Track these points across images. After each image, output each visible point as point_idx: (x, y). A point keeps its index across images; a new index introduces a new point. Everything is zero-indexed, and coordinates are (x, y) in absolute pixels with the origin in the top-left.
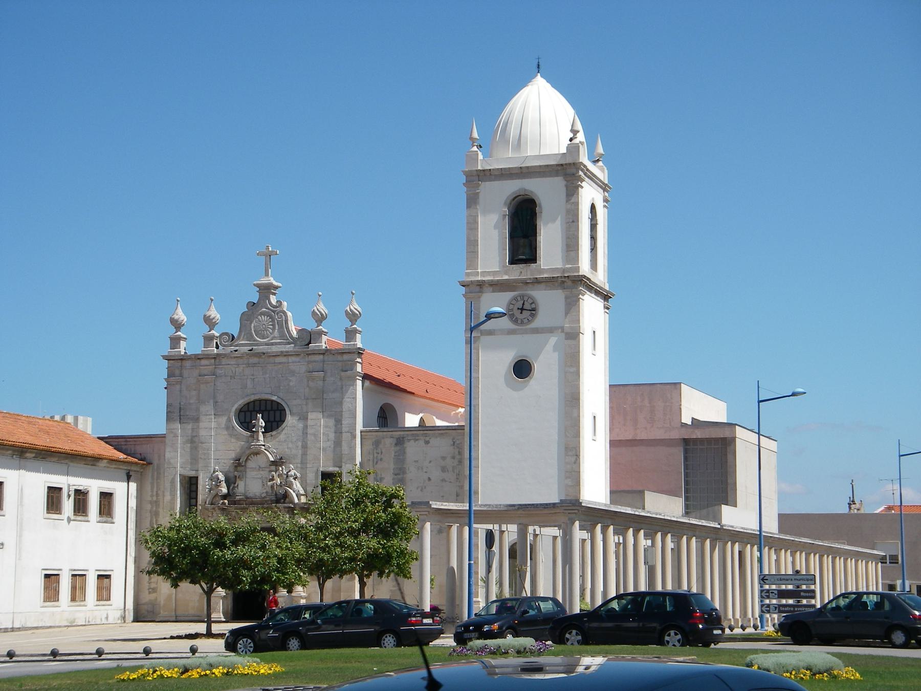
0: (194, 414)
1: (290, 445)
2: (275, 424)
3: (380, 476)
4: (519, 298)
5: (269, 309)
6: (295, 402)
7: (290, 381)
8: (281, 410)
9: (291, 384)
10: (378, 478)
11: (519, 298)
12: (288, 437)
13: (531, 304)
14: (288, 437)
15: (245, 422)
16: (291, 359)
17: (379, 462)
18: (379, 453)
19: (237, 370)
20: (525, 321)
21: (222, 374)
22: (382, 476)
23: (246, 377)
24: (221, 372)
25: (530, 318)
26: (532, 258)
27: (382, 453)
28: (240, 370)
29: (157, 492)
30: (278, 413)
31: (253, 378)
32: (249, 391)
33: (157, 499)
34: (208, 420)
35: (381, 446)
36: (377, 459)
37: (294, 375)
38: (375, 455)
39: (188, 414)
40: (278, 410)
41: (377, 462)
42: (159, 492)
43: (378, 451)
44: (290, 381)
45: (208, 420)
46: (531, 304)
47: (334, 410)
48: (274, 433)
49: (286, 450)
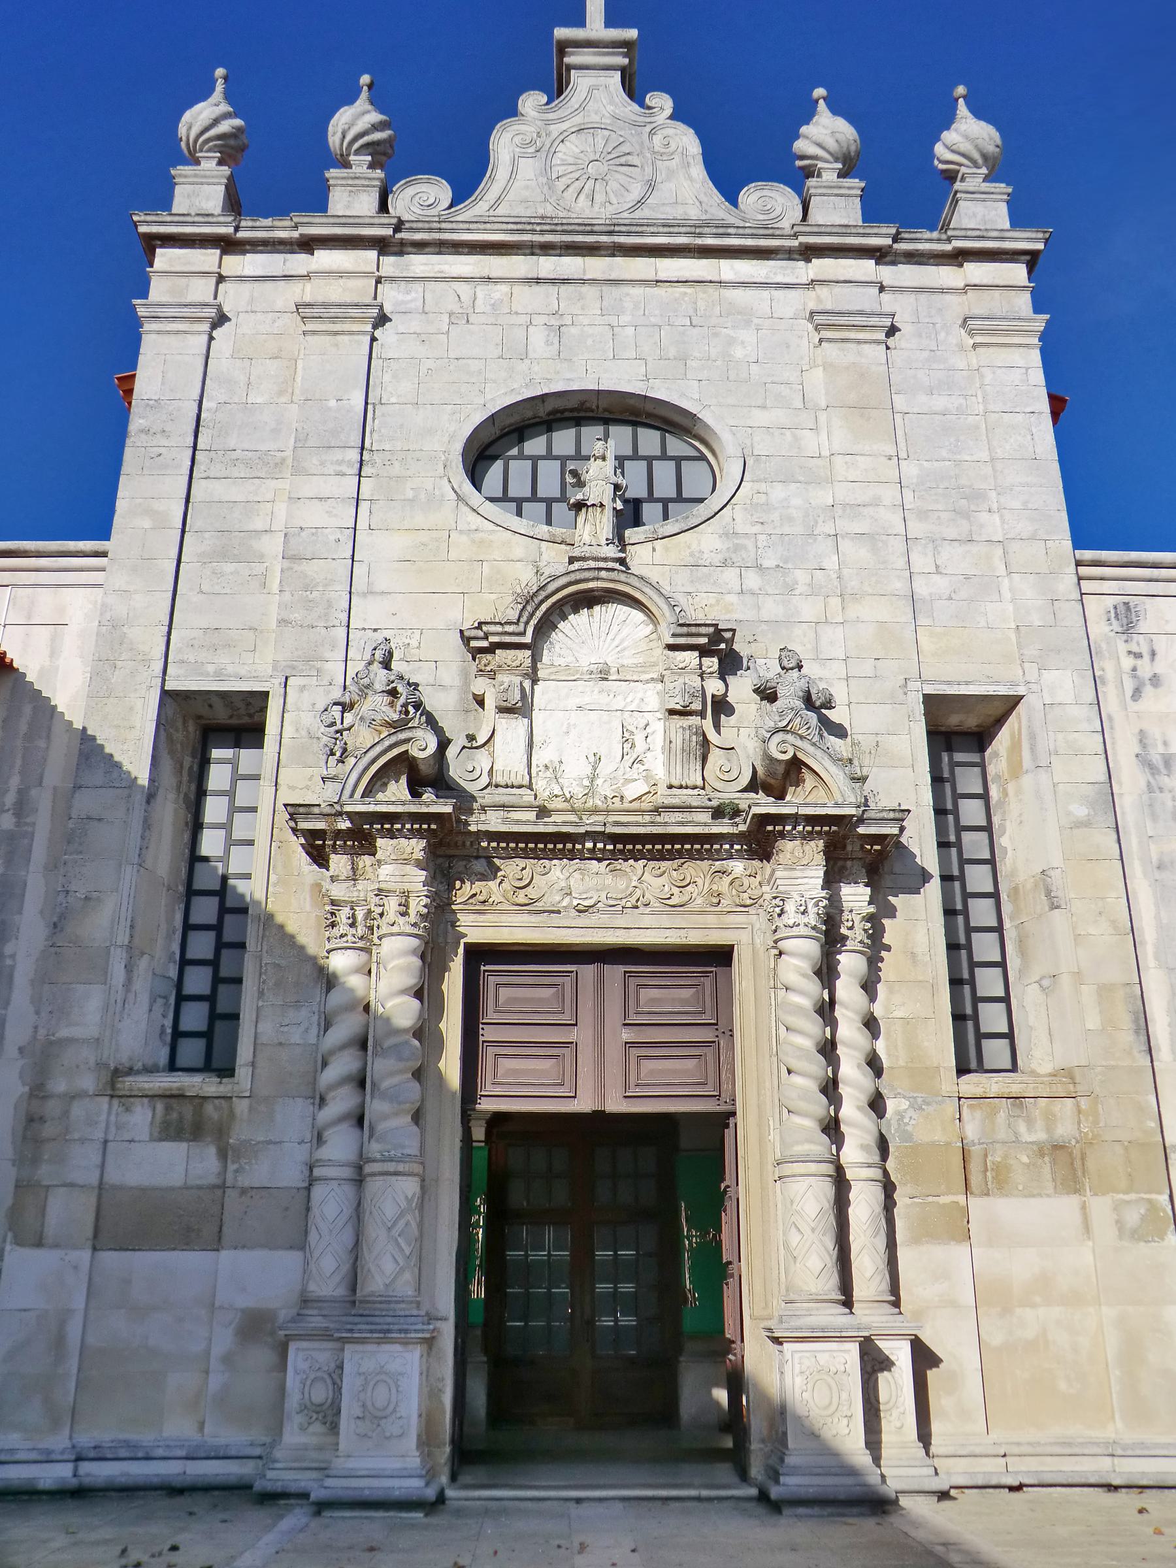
0: (263, 447)
1: (753, 580)
3: (1161, 749)
6: (760, 418)
7: (731, 341)
8: (678, 460)
9: (738, 353)
10: (1157, 760)
12: (737, 548)
14: (737, 548)
17: (1148, 690)
18: (1138, 656)
19: (480, 295)
21: (412, 305)
23: (524, 319)
24: (400, 297)
27: (1153, 654)
28: (497, 296)
29: (22, 793)
30: (664, 473)
31: (554, 321)
32: (536, 368)
33: (18, 824)
34: (331, 469)
35: (1143, 627)
36: (1135, 677)
37: (748, 322)
38: (1127, 662)
39: (232, 443)
40: (664, 457)
41: (1137, 693)
42: (34, 792)
43: (1135, 649)
44: (731, 341)
45: (331, 469)
47: (944, 453)
48: (670, 527)
49: (732, 598)
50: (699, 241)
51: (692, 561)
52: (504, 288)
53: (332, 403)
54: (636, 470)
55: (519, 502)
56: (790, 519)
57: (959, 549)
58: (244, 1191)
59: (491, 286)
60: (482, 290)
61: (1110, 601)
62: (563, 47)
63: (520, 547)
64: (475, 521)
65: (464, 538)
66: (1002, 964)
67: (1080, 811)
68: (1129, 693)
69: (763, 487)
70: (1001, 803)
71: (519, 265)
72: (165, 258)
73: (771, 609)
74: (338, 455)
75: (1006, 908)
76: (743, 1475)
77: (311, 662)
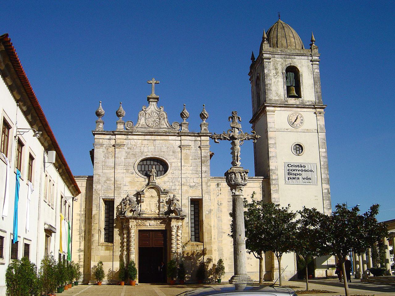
2: (159, 173)
4: (294, 114)
5: (156, 110)
11: (294, 114)
13: (301, 117)
15: (141, 171)
16: (170, 138)
20: (298, 125)
22: (222, 203)
25: (301, 124)
26: (299, 96)
27: (221, 190)
38: (217, 191)
39: (107, 164)
46: (301, 117)
48: (162, 176)
50: (166, 134)
51: (164, 181)
52: (141, 140)
53: (119, 159)
54: (157, 166)
55: (143, 171)
56: (176, 175)
57: (196, 179)
58: (115, 256)
59: (139, 140)
60: (138, 141)
61: (216, 183)
62: (148, 99)
63: (143, 180)
64: (138, 176)
65: (137, 178)
66: (199, 229)
67: (208, 213)
68: (217, 195)
69: (173, 171)
70: (200, 210)
71: (143, 137)
72: (96, 136)
73: (173, 188)
74: (120, 166)
75: (199, 222)
76: (167, 282)
77: (119, 194)
